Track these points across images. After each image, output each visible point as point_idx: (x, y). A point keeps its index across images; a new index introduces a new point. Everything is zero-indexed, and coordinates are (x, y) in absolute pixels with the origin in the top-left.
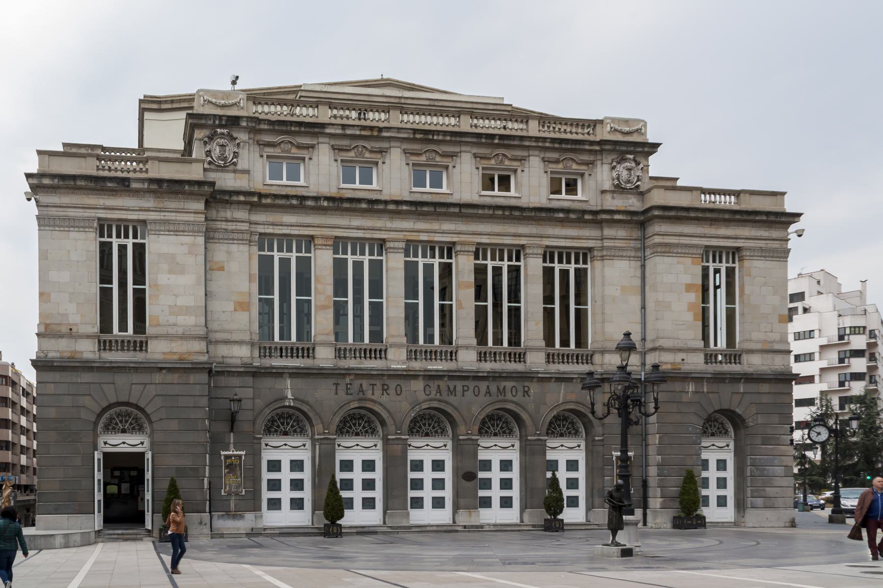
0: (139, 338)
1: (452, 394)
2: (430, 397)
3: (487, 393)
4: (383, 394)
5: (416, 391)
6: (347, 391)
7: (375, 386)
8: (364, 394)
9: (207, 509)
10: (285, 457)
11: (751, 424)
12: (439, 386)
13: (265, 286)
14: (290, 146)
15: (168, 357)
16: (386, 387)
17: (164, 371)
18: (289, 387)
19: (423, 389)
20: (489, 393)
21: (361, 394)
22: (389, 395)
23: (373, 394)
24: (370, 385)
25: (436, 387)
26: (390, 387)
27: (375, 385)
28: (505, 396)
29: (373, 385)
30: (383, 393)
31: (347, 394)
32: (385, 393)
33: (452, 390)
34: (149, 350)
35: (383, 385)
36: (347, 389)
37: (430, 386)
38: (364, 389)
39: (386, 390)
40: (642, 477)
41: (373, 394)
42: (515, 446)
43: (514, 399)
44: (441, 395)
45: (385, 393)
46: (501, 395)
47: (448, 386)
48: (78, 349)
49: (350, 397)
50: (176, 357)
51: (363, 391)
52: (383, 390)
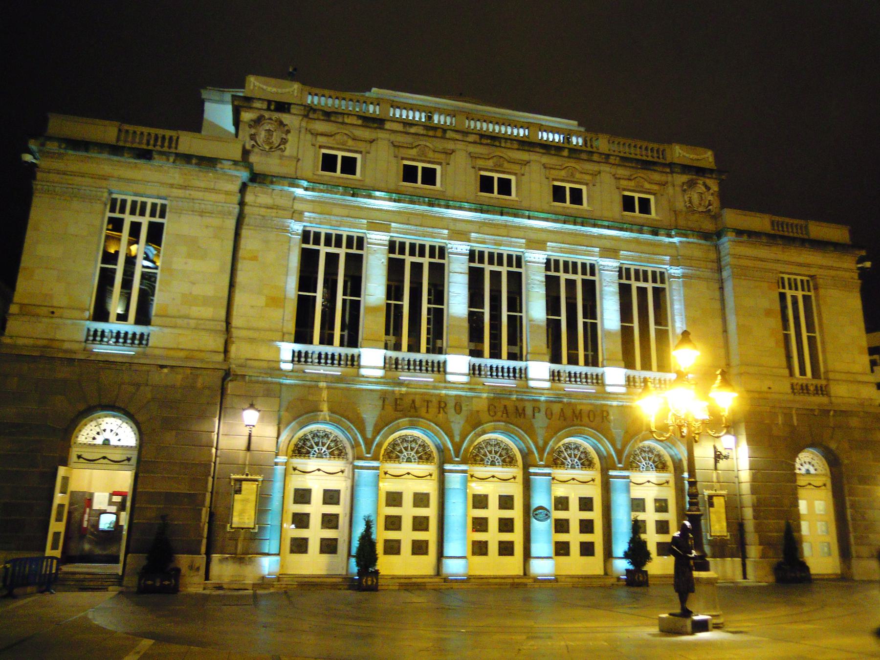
0: (139, 329)
1: (520, 416)
2: (495, 418)
3: (560, 416)
4: (439, 413)
5: (478, 412)
6: (396, 407)
7: (430, 404)
8: (416, 412)
9: (203, 549)
10: (317, 485)
11: (846, 462)
12: (505, 407)
13: (307, 281)
14: (345, 137)
15: (172, 353)
16: (443, 405)
17: (165, 370)
18: (325, 399)
19: (486, 409)
20: (564, 416)
21: (413, 410)
22: (446, 413)
23: (427, 412)
24: (424, 401)
25: (502, 408)
26: (448, 405)
27: (431, 401)
28: (581, 421)
29: (428, 402)
30: (439, 410)
31: (396, 410)
32: (442, 411)
33: (520, 411)
34: (150, 344)
35: (440, 402)
36: (396, 404)
37: (495, 407)
38: (417, 406)
39: (443, 408)
40: (738, 519)
41: (427, 412)
42: (596, 480)
43: (593, 424)
44: (508, 417)
45: (442, 411)
46: (577, 419)
47: (516, 407)
48: (58, 337)
49: (399, 414)
50: (182, 354)
51: (415, 408)
52: (440, 407)
